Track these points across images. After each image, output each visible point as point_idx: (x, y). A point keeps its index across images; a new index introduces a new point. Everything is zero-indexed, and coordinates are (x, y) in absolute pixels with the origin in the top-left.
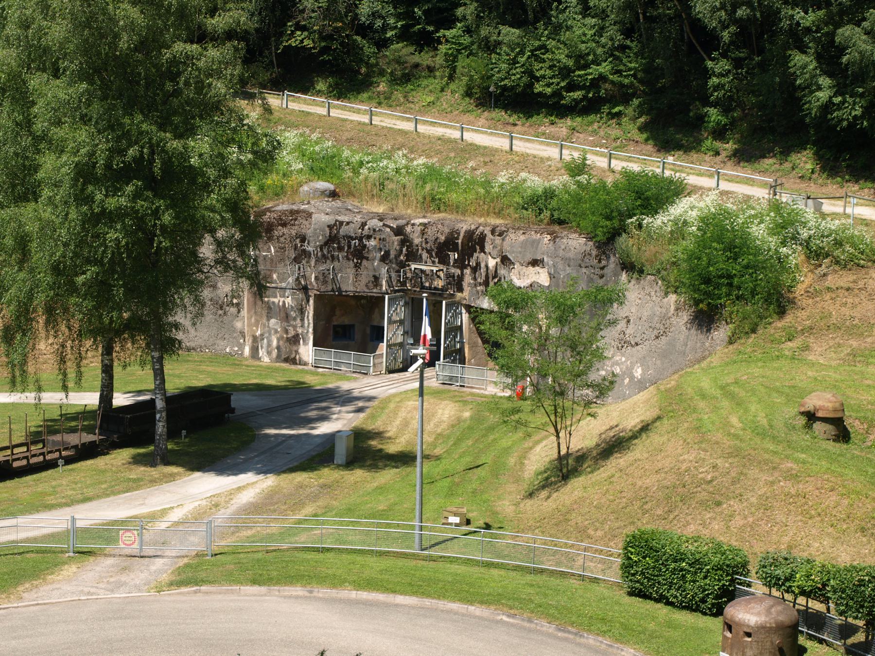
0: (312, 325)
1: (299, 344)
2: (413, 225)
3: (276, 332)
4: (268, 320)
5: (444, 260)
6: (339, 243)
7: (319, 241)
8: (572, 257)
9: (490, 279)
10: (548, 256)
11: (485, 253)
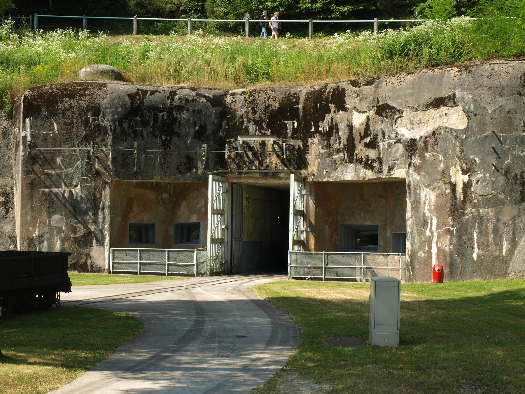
0: (108, 220)
1: (92, 246)
2: (233, 94)
3: (60, 231)
4: (50, 217)
5: (278, 130)
6: (142, 116)
7: (118, 114)
8: (504, 83)
9: (357, 142)
10: (463, 89)
11: (345, 110)
